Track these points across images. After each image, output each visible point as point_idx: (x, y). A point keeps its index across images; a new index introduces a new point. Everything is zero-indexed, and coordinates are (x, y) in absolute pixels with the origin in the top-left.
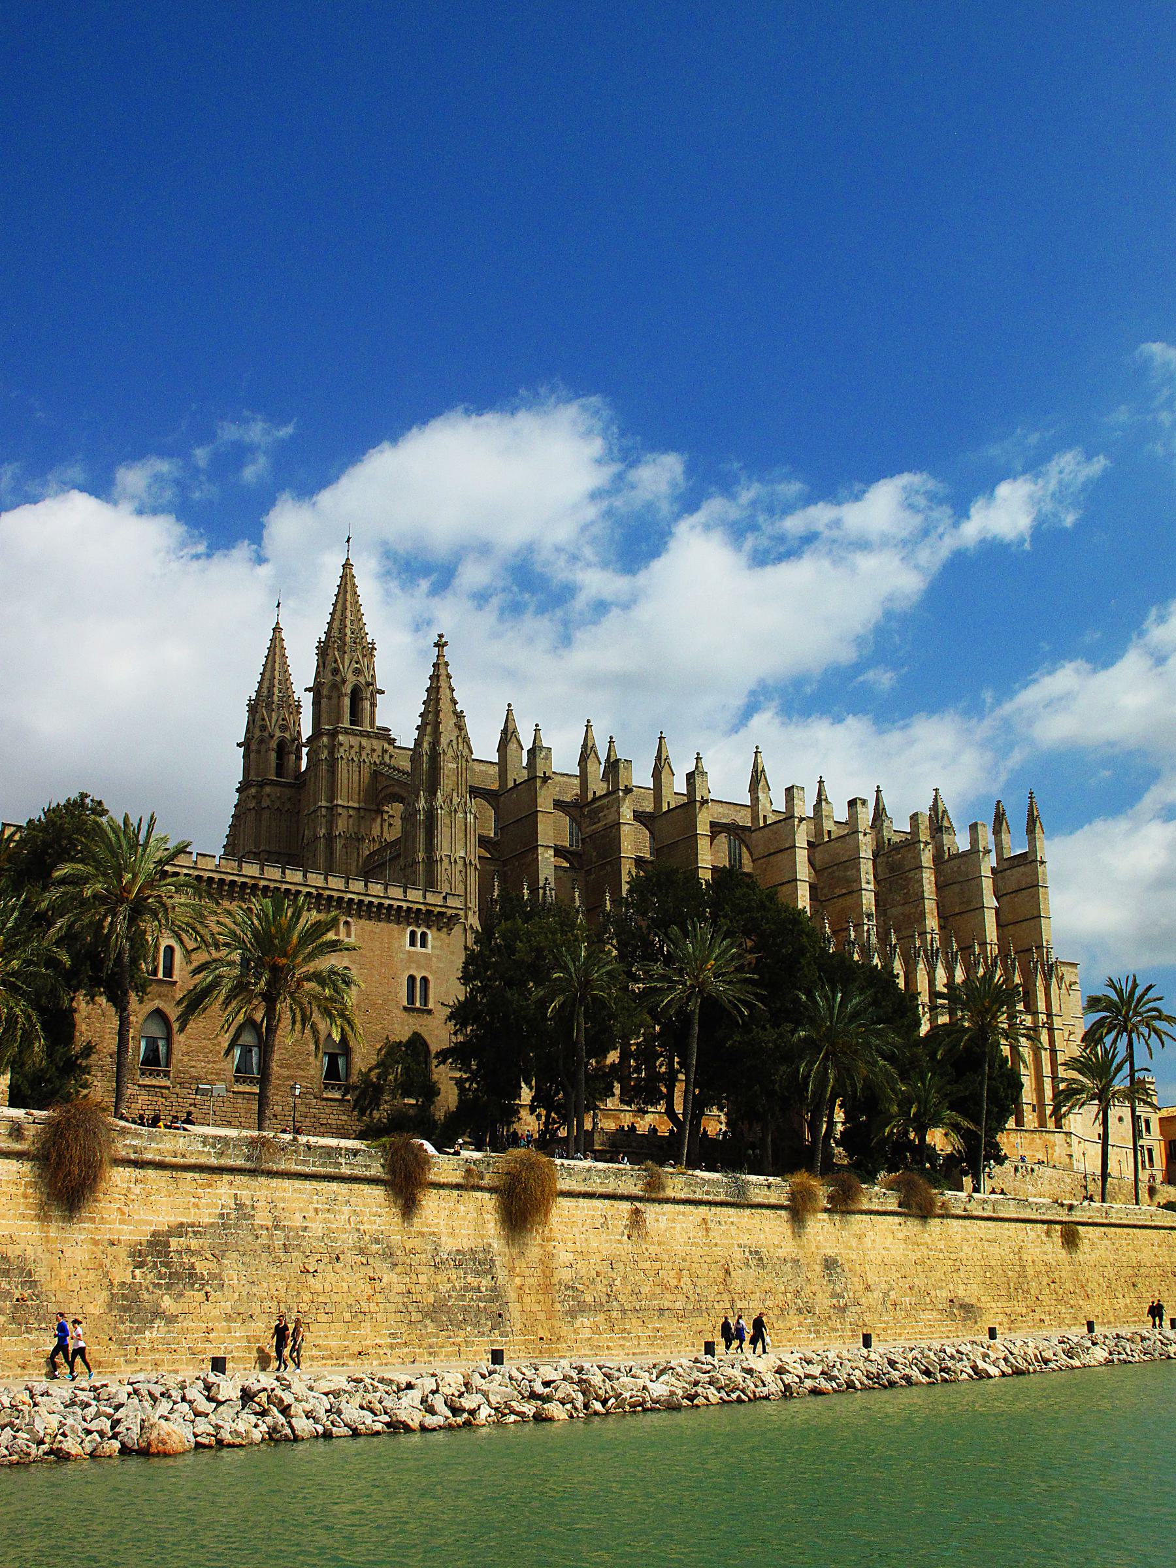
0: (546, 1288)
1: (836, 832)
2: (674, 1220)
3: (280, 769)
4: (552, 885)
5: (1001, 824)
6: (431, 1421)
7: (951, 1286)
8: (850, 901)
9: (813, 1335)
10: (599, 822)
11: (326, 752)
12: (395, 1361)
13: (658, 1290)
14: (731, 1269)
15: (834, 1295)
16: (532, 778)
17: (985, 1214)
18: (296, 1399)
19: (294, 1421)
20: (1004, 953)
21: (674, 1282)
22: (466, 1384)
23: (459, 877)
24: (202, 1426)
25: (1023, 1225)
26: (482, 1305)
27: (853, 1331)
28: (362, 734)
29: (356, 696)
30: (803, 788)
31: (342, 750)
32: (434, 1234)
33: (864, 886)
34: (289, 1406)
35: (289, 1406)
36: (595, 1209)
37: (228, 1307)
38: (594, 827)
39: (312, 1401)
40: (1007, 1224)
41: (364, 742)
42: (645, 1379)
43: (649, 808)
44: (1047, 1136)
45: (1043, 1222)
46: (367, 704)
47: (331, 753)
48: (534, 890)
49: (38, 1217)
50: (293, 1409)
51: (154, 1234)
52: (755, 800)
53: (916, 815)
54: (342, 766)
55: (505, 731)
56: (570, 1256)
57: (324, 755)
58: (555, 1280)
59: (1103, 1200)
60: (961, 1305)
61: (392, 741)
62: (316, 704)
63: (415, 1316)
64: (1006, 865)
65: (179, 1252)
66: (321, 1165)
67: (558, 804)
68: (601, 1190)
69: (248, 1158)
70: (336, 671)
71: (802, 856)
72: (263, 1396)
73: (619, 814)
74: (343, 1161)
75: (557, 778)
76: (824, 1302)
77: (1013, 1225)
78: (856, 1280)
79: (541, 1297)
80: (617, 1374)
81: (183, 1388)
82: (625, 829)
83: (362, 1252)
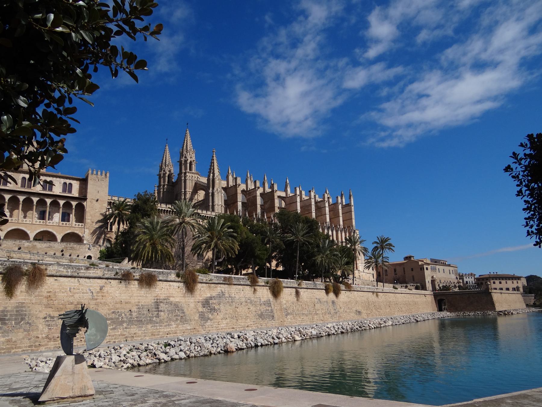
0: (281, 310)
8: (309, 215)
9: (331, 319)
15: (335, 310)
16: (236, 185)
20: (344, 228)
23: (220, 209)
28: (192, 173)
31: (187, 177)
33: (313, 211)
36: (289, 290)
40: (365, 293)
41: (193, 175)
45: (372, 292)
48: (237, 212)
49: (183, 297)
51: (206, 300)
54: (188, 182)
59: (377, 286)
63: (258, 317)
64: (344, 206)
65: (212, 304)
71: (299, 204)
72: (242, 336)
74: (241, 281)
76: (333, 311)
78: (338, 306)
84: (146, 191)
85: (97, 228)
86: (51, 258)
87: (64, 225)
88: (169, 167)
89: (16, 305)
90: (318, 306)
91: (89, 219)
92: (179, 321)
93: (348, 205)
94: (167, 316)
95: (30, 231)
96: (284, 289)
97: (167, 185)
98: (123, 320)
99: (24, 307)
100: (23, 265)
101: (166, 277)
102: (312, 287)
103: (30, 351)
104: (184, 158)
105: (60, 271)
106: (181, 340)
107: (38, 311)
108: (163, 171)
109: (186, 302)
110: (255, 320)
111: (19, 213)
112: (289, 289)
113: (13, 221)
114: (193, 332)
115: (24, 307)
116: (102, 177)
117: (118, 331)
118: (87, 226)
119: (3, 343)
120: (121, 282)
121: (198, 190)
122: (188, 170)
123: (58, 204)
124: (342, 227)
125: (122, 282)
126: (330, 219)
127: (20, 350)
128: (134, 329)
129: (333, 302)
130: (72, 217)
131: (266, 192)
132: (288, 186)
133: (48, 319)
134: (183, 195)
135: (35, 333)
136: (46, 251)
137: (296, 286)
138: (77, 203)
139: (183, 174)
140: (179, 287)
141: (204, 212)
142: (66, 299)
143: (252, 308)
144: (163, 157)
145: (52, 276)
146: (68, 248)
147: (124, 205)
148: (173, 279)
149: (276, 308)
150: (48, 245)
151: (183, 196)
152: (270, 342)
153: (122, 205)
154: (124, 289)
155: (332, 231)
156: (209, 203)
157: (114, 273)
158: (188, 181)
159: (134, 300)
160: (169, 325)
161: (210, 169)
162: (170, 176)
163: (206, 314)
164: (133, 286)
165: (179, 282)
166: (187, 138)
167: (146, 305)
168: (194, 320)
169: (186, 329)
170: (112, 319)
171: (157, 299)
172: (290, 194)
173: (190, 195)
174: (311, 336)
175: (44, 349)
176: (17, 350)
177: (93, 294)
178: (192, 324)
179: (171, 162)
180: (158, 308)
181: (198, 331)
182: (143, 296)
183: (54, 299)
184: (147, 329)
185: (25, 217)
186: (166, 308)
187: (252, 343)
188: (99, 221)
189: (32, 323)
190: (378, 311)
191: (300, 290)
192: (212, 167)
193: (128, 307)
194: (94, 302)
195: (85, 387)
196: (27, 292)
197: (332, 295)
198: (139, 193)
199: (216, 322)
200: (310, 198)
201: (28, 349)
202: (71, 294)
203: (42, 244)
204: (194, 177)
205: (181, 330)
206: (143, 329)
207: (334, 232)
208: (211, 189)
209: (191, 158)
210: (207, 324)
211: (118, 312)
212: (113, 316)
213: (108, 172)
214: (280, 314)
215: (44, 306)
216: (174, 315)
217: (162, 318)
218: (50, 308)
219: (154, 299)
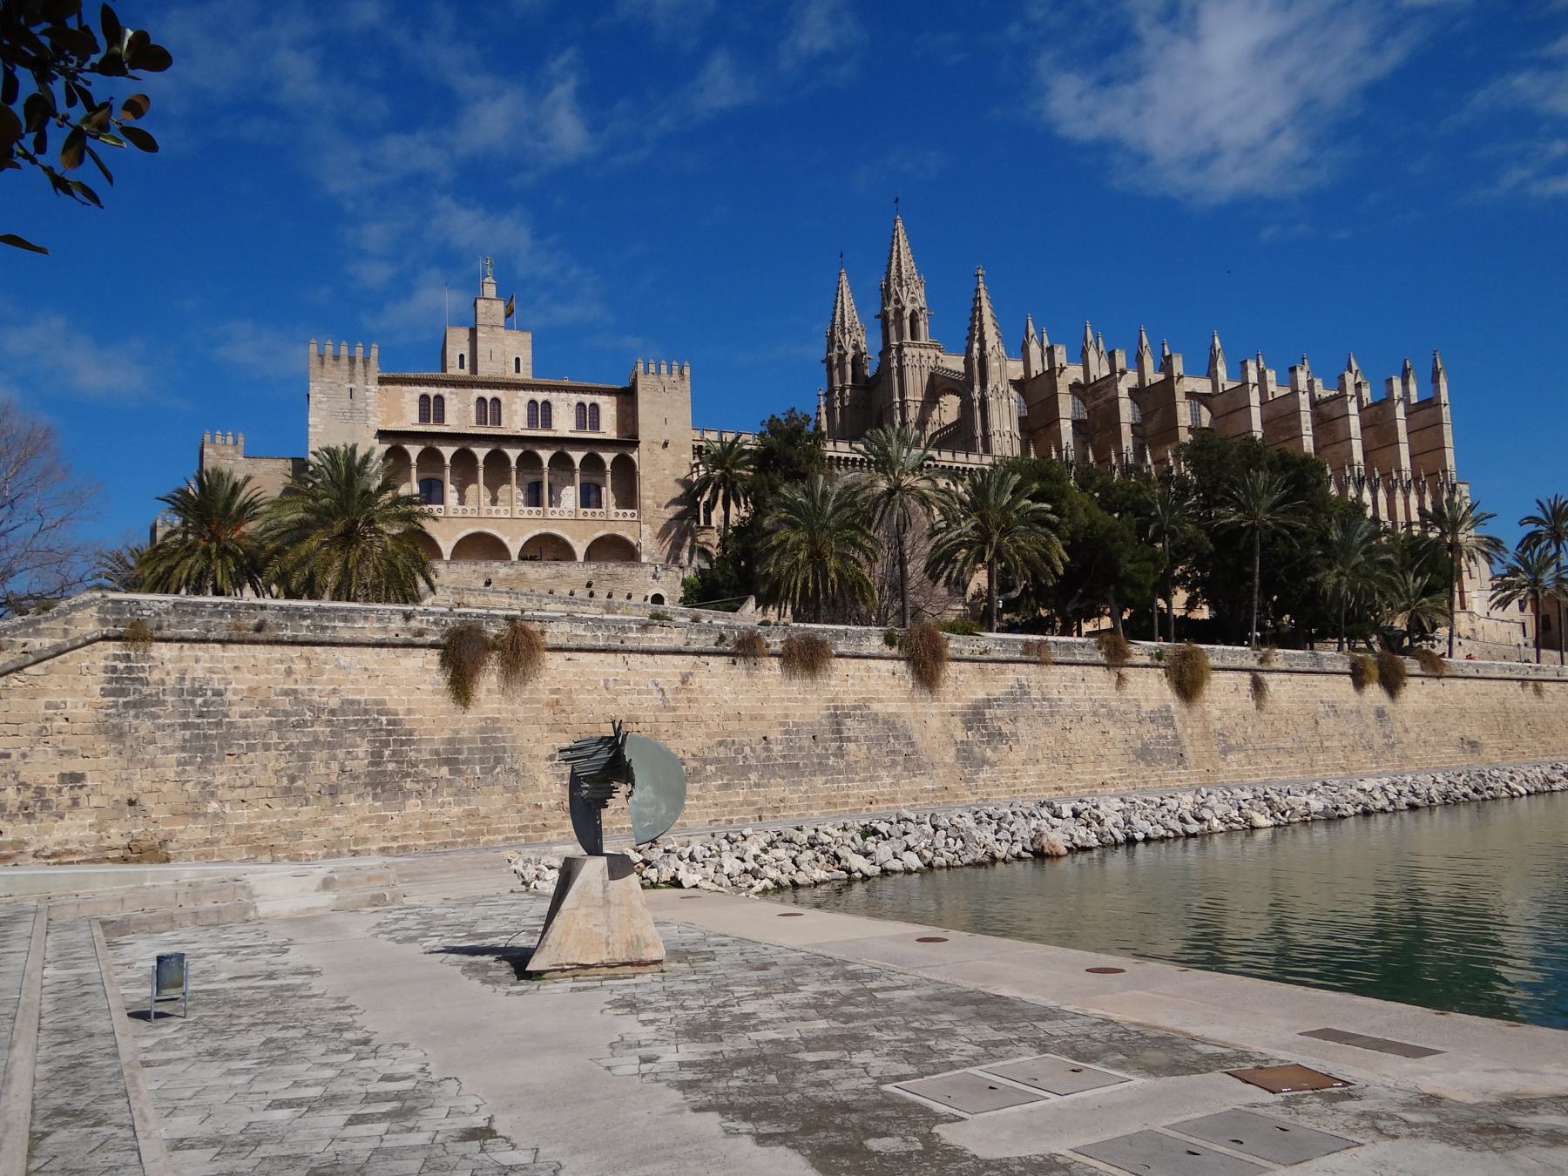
0: (1206, 735)
4: (1072, 447)
5: (1408, 377)
7: (1461, 729)
9: (1374, 765)
10: (1101, 397)
15: (1386, 736)
16: (1052, 369)
17: (1479, 675)
20: (1416, 478)
23: (1007, 446)
26: (1170, 748)
27: (1400, 761)
31: (907, 359)
33: (1304, 432)
36: (1230, 679)
37: (1023, 755)
38: (1096, 402)
40: (1493, 682)
41: (923, 352)
45: (1518, 680)
51: (975, 707)
54: (909, 372)
58: (1211, 730)
59: (1538, 662)
60: (1469, 743)
63: (1132, 757)
64: (1413, 409)
68: (1232, 665)
69: (1022, 653)
71: (1256, 414)
72: (1086, 813)
74: (1076, 651)
76: (1379, 741)
77: (1498, 683)
78: (1398, 724)
84: (793, 410)
85: (671, 520)
87: (589, 517)
88: (854, 335)
90: (1327, 725)
91: (648, 498)
92: (899, 768)
93: (1430, 403)
94: (865, 754)
96: (1215, 676)
97: (851, 388)
98: (747, 762)
99: (500, 729)
100: (487, 623)
101: (856, 646)
102: (1307, 668)
104: (892, 303)
105: (576, 635)
106: (906, 820)
107: (533, 739)
108: (836, 349)
109: (916, 714)
111: (478, 491)
113: (468, 515)
114: (942, 797)
116: (673, 379)
117: (738, 793)
118: (646, 515)
120: (734, 663)
121: (940, 395)
122: (908, 339)
123: (570, 461)
124: (1409, 474)
125: (738, 661)
126: (1365, 453)
127: (500, 838)
128: (778, 789)
129: (1380, 713)
130: (607, 494)
131: (1147, 384)
132: (1220, 359)
134: (898, 412)
135: (529, 797)
136: (550, 587)
137: (1254, 664)
138: (615, 454)
139: (894, 351)
140: (894, 674)
141: (961, 457)
142: (598, 709)
143: (1115, 732)
144: (835, 308)
147: (735, 453)
148: (875, 652)
149: (1189, 730)
150: (554, 571)
151: (899, 416)
152: (1174, 831)
153: (731, 453)
154: (744, 679)
155: (1374, 492)
156: (973, 429)
157: (714, 637)
158: (910, 372)
159: (773, 711)
160: (872, 778)
161: (971, 328)
162: (857, 362)
163: (976, 749)
164: (766, 673)
165: (893, 658)
166: (898, 244)
169: (921, 791)
170: (717, 761)
171: (836, 708)
172: (1225, 381)
173: (918, 410)
174: (1307, 815)
175: (555, 838)
176: (492, 838)
177: (664, 694)
178: (937, 775)
179: (856, 319)
180: (839, 732)
181: (957, 796)
182: (796, 700)
183: (568, 709)
184: (814, 788)
185: (494, 501)
187: (1116, 832)
188: (675, 502)
190: (1543, 739)
192: (977, 323)
193: (759, 728)
194: (666, 716)
195: (638, 940)
196: (503, 692)
197: (1374, 692)
198: (773, 416)
199: (1009, 771)
200: (1295, 391)
201: (517, 835)
204: (925, 358)
205: (907, 793)
206: (801, 788)
207: (1382, 494)
208: (977, 388)
209: (913, 300)
210: (981, 775)
211: (733, 742)
212: (721, 752)
213: (686, 363)
215: (545, 728)
216: (885, 750)
217: (852, 758)
218: (561, 731)
219: (828, 708)
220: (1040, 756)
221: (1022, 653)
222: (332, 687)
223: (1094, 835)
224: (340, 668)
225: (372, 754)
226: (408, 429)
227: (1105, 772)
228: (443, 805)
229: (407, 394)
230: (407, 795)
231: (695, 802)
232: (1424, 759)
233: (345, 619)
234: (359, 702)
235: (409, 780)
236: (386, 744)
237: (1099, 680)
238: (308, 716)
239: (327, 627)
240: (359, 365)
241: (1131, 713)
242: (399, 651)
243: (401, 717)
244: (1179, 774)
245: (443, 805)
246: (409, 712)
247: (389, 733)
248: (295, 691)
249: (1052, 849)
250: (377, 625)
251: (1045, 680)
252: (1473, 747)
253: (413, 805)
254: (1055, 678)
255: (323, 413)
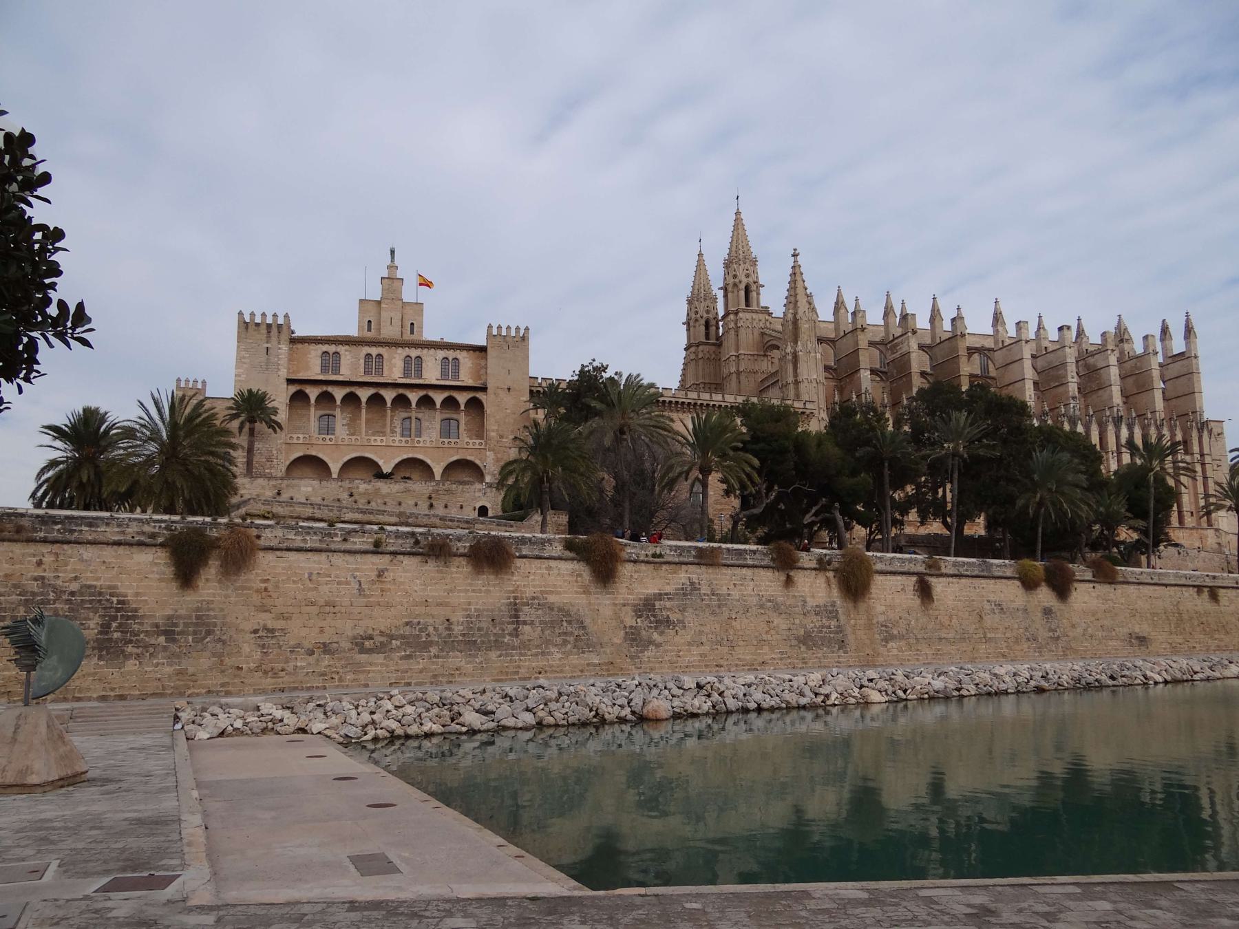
0: (869, 626)
1: (1051, 347)
2: (946, 587)
3: (707, 336)
5: (1166, 334)
6: (803, 701)
7: (1130, 625)
8: (1061, 389)
9: (1037, 654)
11: (733, 323)
12: (783, 667)
13: (938, 627)
14: (983, 615)
15: (1051, 630)
17: (1153, 582)
18: (727, 688)
19: (726, 699)
21: (948, 623)
22: (823, 681)
23: (814, 391)
24: (676, 703)
25: (1179, 588)
26: (832, 635)
28: (752, 311)
29: (747, 290)
30: (1027, 322)
32: (802, 596)
33: (1070, 380)
34: (723, 692)
35: (723, 692)
36: (898, 581)
37: (689, 638)
39: (736, 689)
41: (755, 316)
42: (929, 678)
43: (928, 341)
44: (1202, 531)
45: (1194, 586)
46: (754, 294)
47: (736, 324)
48: (859, 396)
50: (725, 693)
51: (646, 600)
52: (996, 331)
53: (1105, 333)
54: (742, 331)
55: (837, 303)
56: (883, 608)
57: (732, 325)
61: (770, 314)
62: (726, 296)
63: (794, 642)
64: (1170, 361)
66: (737, 560)
67: (871, 344)
69: (695, 557)
70: (735, 276)
72: (709, 687)
73: (909, 346)
74: (748, 557)
75: (871, 328)
76: (1043, 634)
77: (1173, 588)
79: (867, 631)
80: (912, 676)
81: (665, 682)
82: (913, 356)
83: (762, 607)
86: (357, 514)
87: (446, 445)
89: (195, 606)
90: (988, 621)
91: (493, 431)
92: (569, 646)
95: (383, 461)
96: (879, 579)
98: (429, 639)
99: (213, 609)
100: (211, 529)
103: (223, 693)
106: (540, 687)
110: (787, 649)
112: (899, 578)
113: (353, 443)
115: (213, 609)
119: (170, 676)
120: (427, 562)
128: (456, 660)
129: (1047, 612)
133: (261, 633)
137: (921, 568)
143: (780, 622)
145: (272, 549)
146: (440, 492)
149: (852, 622)
150: (402, 487)
152: (788, 702)
160: (543, 654)
163: (644, 633)
167: (488, 610)
168: (610, 645)
169: (588, 665)
170: (403, 637)
171: (515, 598)
176: (196, 691)
177: (360, 585)
178: (605, 653)
180: (517, 616)
182: (480, 591)
186: (538, 617)
189: (228, 640)
190: (1217, 636)
191: (933, 581)
196: (220, 581)
197: (1045, 595)
202: (310, 586)
203: (391, 486)
205: (575, 667)
206: (477, 660)
212: (407, 631)
214: (864, 637)
216: (557, 631)
217: (526, 637)
218: (266, 611)
220: (704, 640)
221: (695, 557)
222: (74, 575)
223: (709, 704)
224: (83, 561)
225: (102, 626)
226: (312, 378)
227: (766, 654)
228: (157, 665)
229: (312, 352)
230: (127, 657)
231: (379, 668)
232: (1089, 650)
233: (90, 525)
234: (95, 587)
235: (130, 645)
236: (115, 618)
237: (768, 582)
238: (52, 596)
239: (75, 530)
240: (274, 330)
241: (797, 606)
242: (135, 549)
243: (129, 598)
244: (839, 657)
245: (157, 665)
246: (137, 594)
247: (118, 610)
248: (43, 578)
249: (655, 714)
250: (117, 530)
251: (716, 579)
252: (1142, 641)
253: (131, 665)
254: (724, 580)
255: (245, 366)
